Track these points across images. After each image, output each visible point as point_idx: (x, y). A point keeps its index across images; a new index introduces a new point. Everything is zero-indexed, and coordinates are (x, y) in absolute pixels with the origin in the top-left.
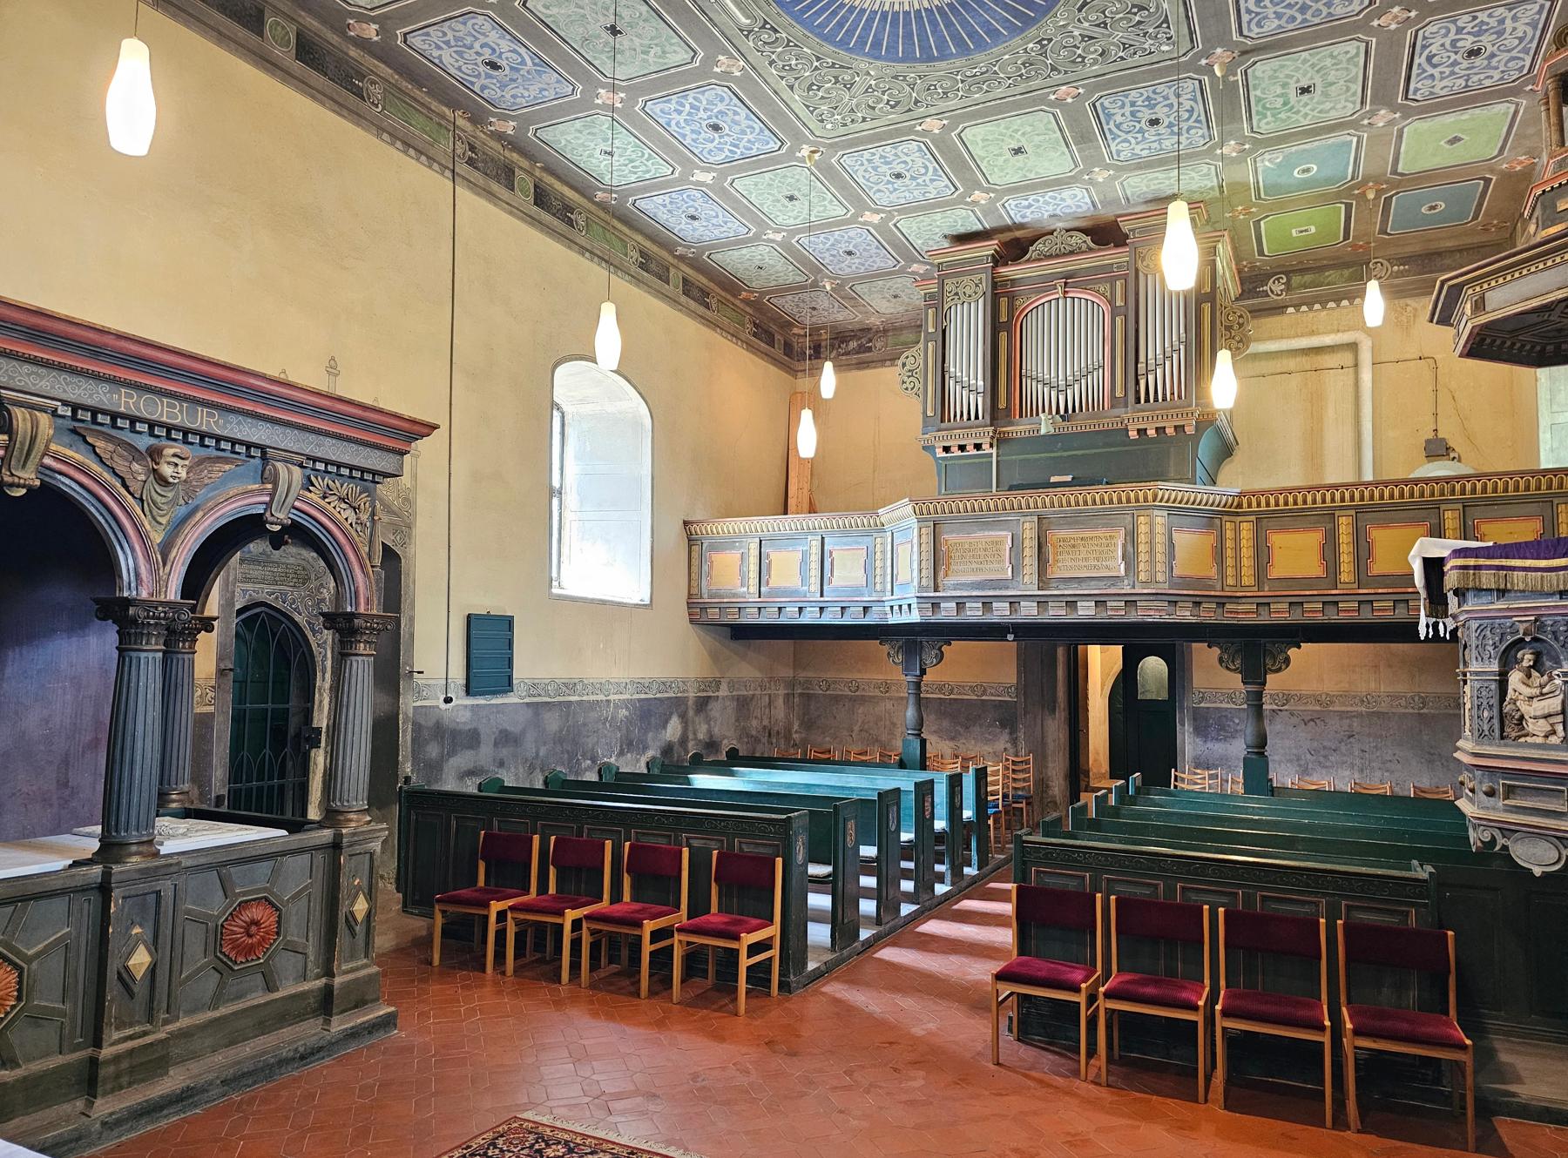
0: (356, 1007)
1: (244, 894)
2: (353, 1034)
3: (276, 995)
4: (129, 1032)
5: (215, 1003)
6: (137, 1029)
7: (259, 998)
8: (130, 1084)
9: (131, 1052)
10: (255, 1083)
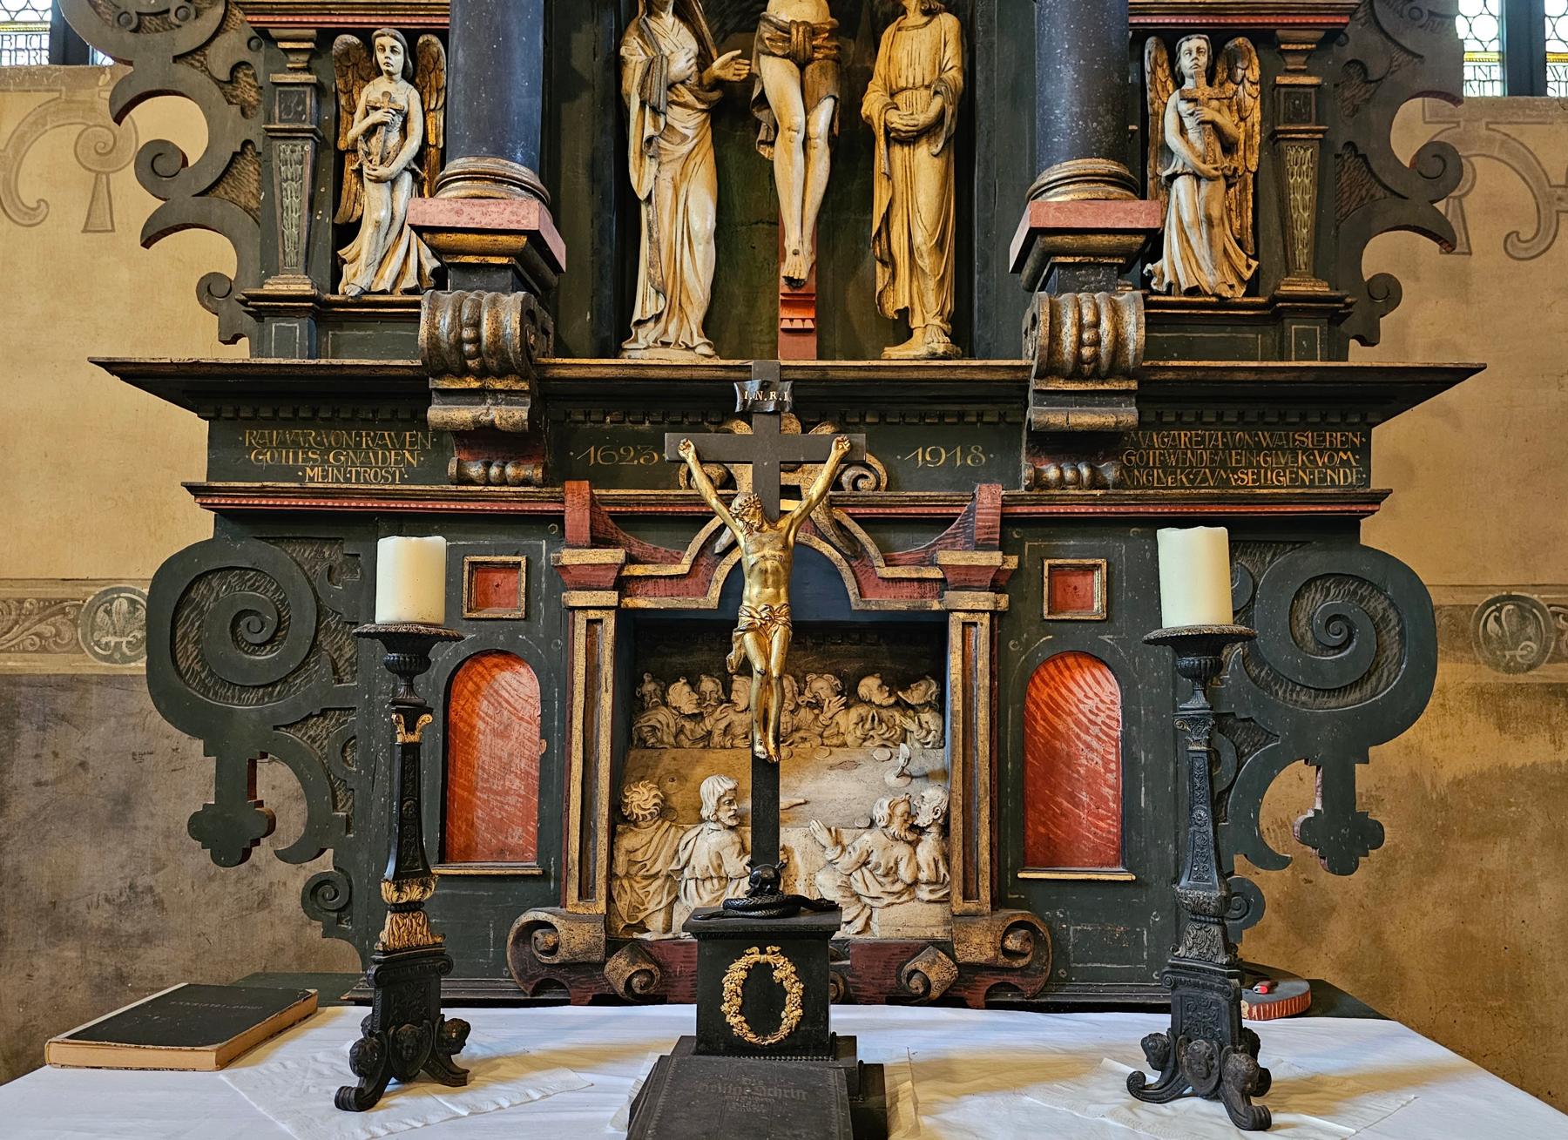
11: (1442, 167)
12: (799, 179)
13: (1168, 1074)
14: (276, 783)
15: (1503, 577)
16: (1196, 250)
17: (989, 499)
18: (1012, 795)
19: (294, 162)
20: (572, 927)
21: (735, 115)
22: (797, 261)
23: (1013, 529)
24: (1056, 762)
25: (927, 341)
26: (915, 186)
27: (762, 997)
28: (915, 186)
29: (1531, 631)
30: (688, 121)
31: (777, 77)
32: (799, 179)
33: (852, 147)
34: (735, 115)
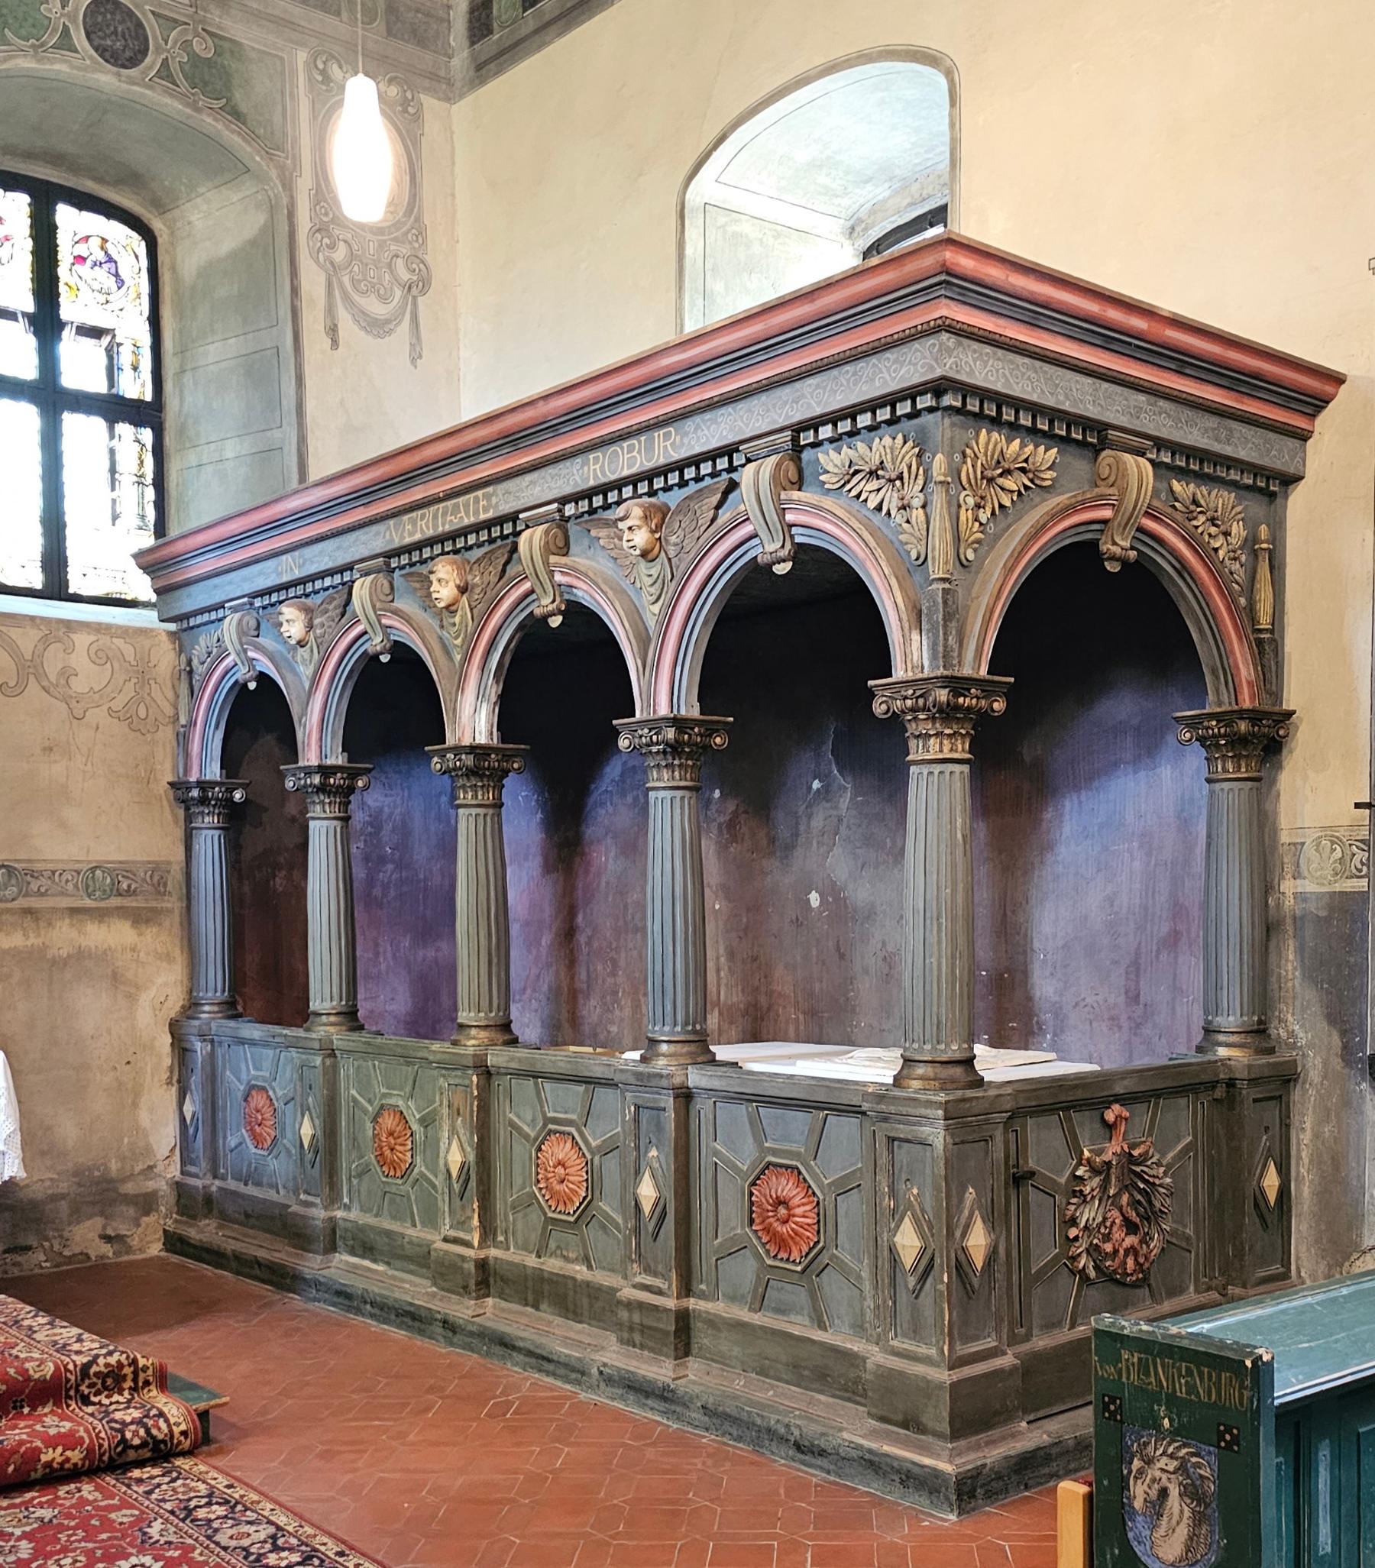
0: (905, 1425)
1: (775, 1152)
2: (874, 1465)
3: (818, 1335)
4: (649, 1280)
5: (760, 1303)
6: (657, 1282)
7: (799, 1326)
8: (642, 1347)
9: (641, 1305)
10: (739, 1439)
29: (13, 881)
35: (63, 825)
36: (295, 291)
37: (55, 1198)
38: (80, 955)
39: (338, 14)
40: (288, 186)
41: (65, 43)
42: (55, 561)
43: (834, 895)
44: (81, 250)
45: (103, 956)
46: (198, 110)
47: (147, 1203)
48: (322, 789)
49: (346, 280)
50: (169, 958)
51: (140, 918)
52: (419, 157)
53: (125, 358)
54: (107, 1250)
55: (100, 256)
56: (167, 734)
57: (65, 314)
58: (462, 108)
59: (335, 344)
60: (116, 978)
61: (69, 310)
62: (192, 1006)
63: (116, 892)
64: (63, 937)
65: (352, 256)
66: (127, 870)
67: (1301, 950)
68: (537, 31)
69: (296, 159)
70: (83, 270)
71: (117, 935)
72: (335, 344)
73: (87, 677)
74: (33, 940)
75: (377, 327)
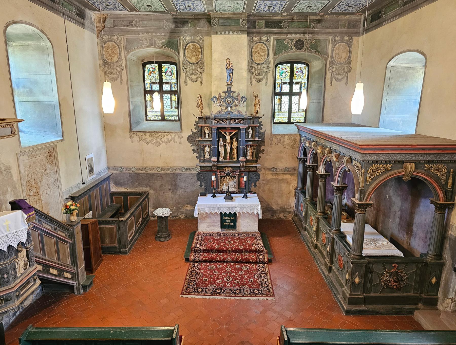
11: (263, 150)
12: (229, 151)
13: (244, 197)
14: (203, 183)
15: (273, 166)
16: (249, 157)
17: (238, 170)
18: (239, 183)
19: (202, 152)
20: (218, 190)
21: (225, 146)
22: (228, 155)
23: (239, 172)
24: (241, 182)
25: (235, 160)
26: (235, 152)
27: (228, 194)
28: (235, 152)
30: (222, 147)
31: (227, 145)
32: (229, 151)
33: (231, 149)
34: (225, 146)
35: (282, 162)
36: (325, 78)
37: (278, 210)
38: (283, 179)
39: (338, 28)
40: (326, 61)
41: (292, 49)
42: (290, 118)
43: (390, 196)
44: (297, 70)
45: (286, 179)
46: (311, 53)
47: (290, 212)
48: (309, 168)
49: (335, 74)
50: (295, 180)
51: (291, 175)
52: (351, 48)
53: (303, 85)
54: (284, 217)
55: (300, 70)
56: (297, 149)
57: (294, 81)
58: (361, 38)
59: (331, 85)
60: (287, 182)
61: (295, 80)
62: (297, 187)
63: (288, 171)
64: (281, 177)
65: (336, 69)
66: (290, 168)
67: (450, 243)
68: (372, 27)
69: (328, 56)
70: (297, 73)
71: (288, 177)
72: (331, 85)
73: (287, 141)
74: (277, 177)
75: (339, 80)
